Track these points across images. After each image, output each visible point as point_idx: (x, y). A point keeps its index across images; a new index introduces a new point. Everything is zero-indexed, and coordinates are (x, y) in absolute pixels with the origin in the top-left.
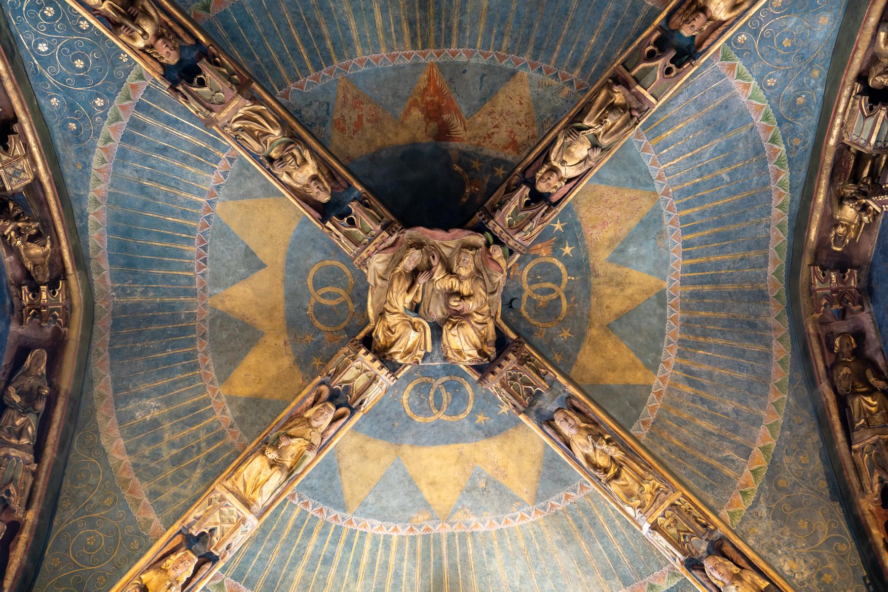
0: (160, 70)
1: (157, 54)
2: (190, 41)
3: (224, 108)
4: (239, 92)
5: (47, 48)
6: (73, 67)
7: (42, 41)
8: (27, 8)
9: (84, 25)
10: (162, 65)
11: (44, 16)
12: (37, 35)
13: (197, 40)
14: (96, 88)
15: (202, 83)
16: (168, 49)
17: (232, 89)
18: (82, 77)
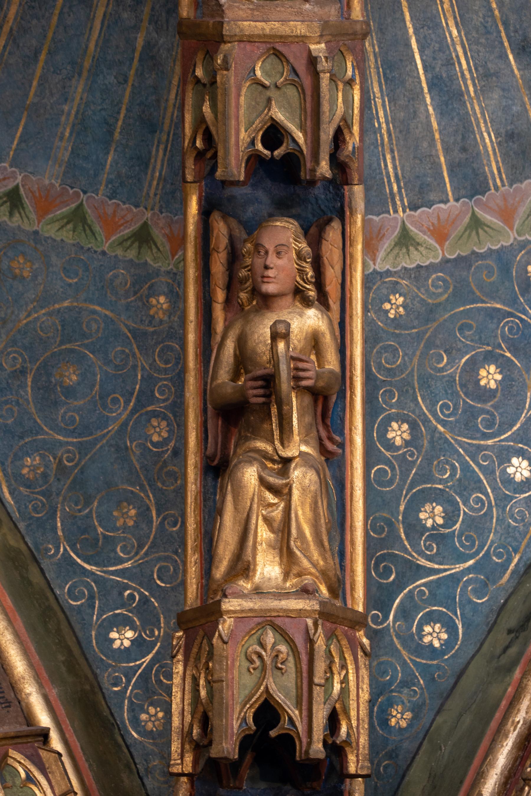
0: (333, 233)
1: (301, 271)
2: (220, 228)
3: (284, 39)
4: (221, 39)
5: (515, 461)
6: (507, 384)
7: (508, 481)
8: (462, 558)
9: (398, 433)
10: (316, 242)
11: (450, 518)
12: (503, 500)
13: (205, 213)
14: (513, 302)
15: (274, 134)
16: (272, 260)
17: (225, 60)
18: (514, 348)
